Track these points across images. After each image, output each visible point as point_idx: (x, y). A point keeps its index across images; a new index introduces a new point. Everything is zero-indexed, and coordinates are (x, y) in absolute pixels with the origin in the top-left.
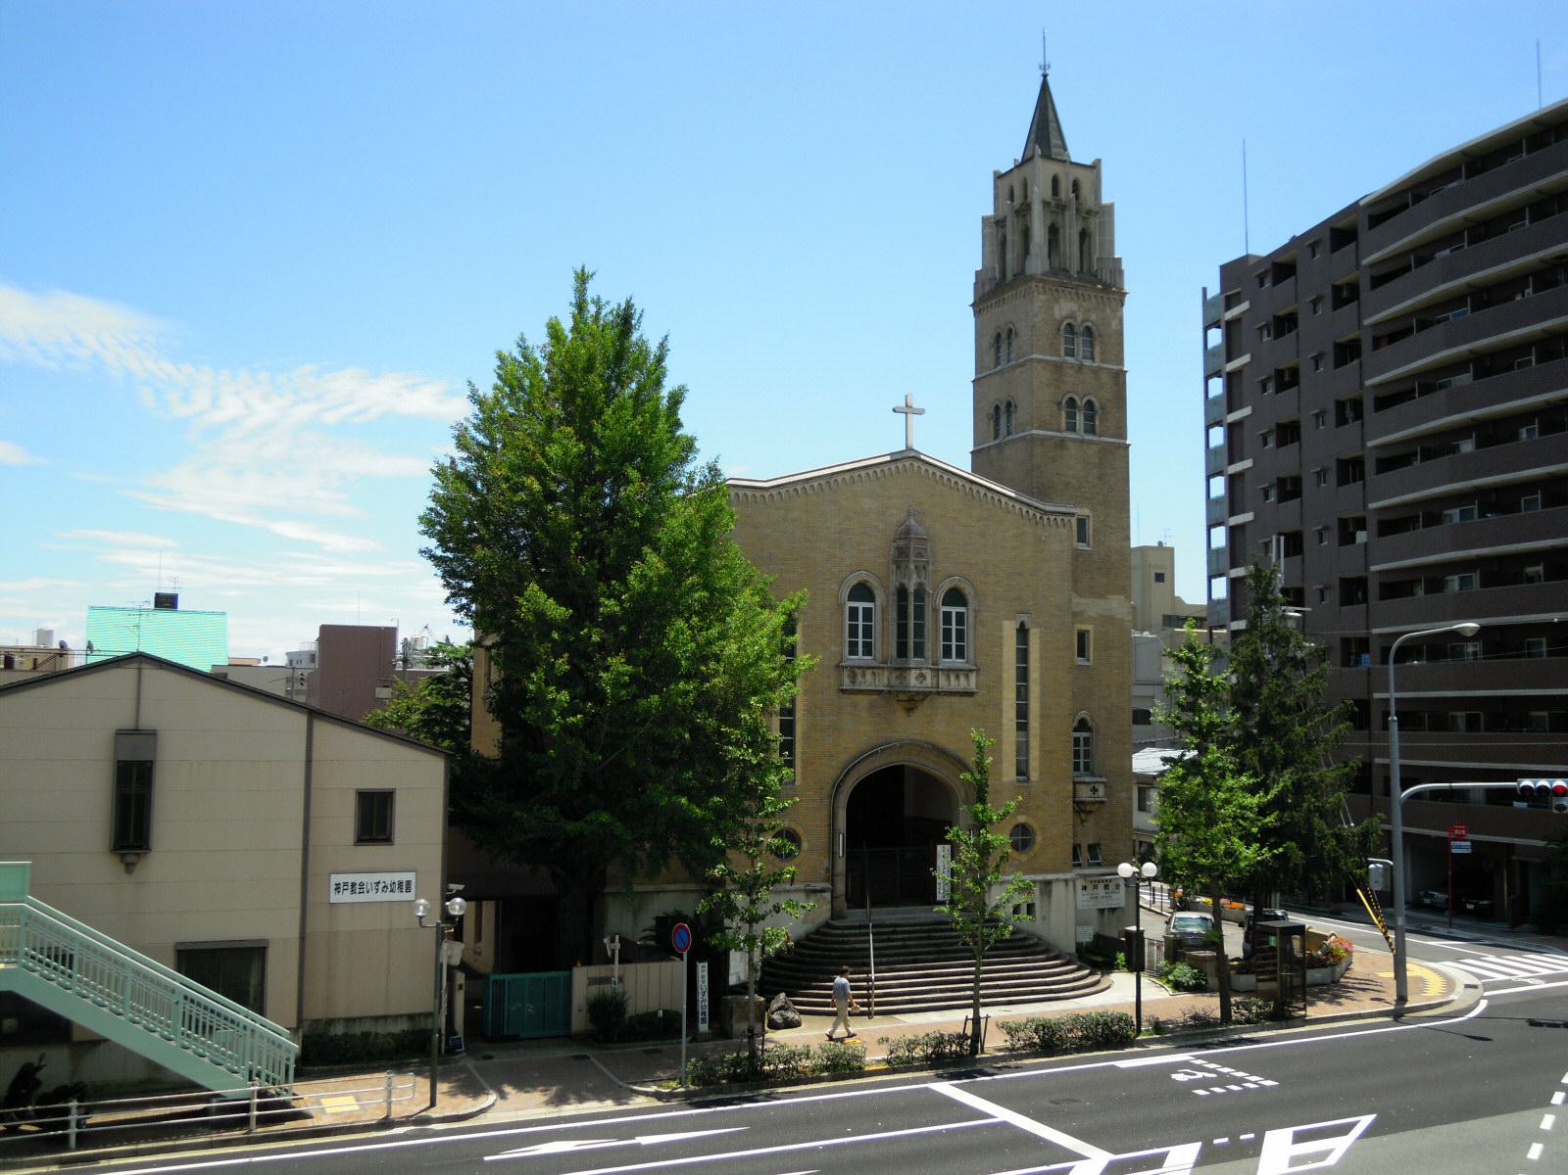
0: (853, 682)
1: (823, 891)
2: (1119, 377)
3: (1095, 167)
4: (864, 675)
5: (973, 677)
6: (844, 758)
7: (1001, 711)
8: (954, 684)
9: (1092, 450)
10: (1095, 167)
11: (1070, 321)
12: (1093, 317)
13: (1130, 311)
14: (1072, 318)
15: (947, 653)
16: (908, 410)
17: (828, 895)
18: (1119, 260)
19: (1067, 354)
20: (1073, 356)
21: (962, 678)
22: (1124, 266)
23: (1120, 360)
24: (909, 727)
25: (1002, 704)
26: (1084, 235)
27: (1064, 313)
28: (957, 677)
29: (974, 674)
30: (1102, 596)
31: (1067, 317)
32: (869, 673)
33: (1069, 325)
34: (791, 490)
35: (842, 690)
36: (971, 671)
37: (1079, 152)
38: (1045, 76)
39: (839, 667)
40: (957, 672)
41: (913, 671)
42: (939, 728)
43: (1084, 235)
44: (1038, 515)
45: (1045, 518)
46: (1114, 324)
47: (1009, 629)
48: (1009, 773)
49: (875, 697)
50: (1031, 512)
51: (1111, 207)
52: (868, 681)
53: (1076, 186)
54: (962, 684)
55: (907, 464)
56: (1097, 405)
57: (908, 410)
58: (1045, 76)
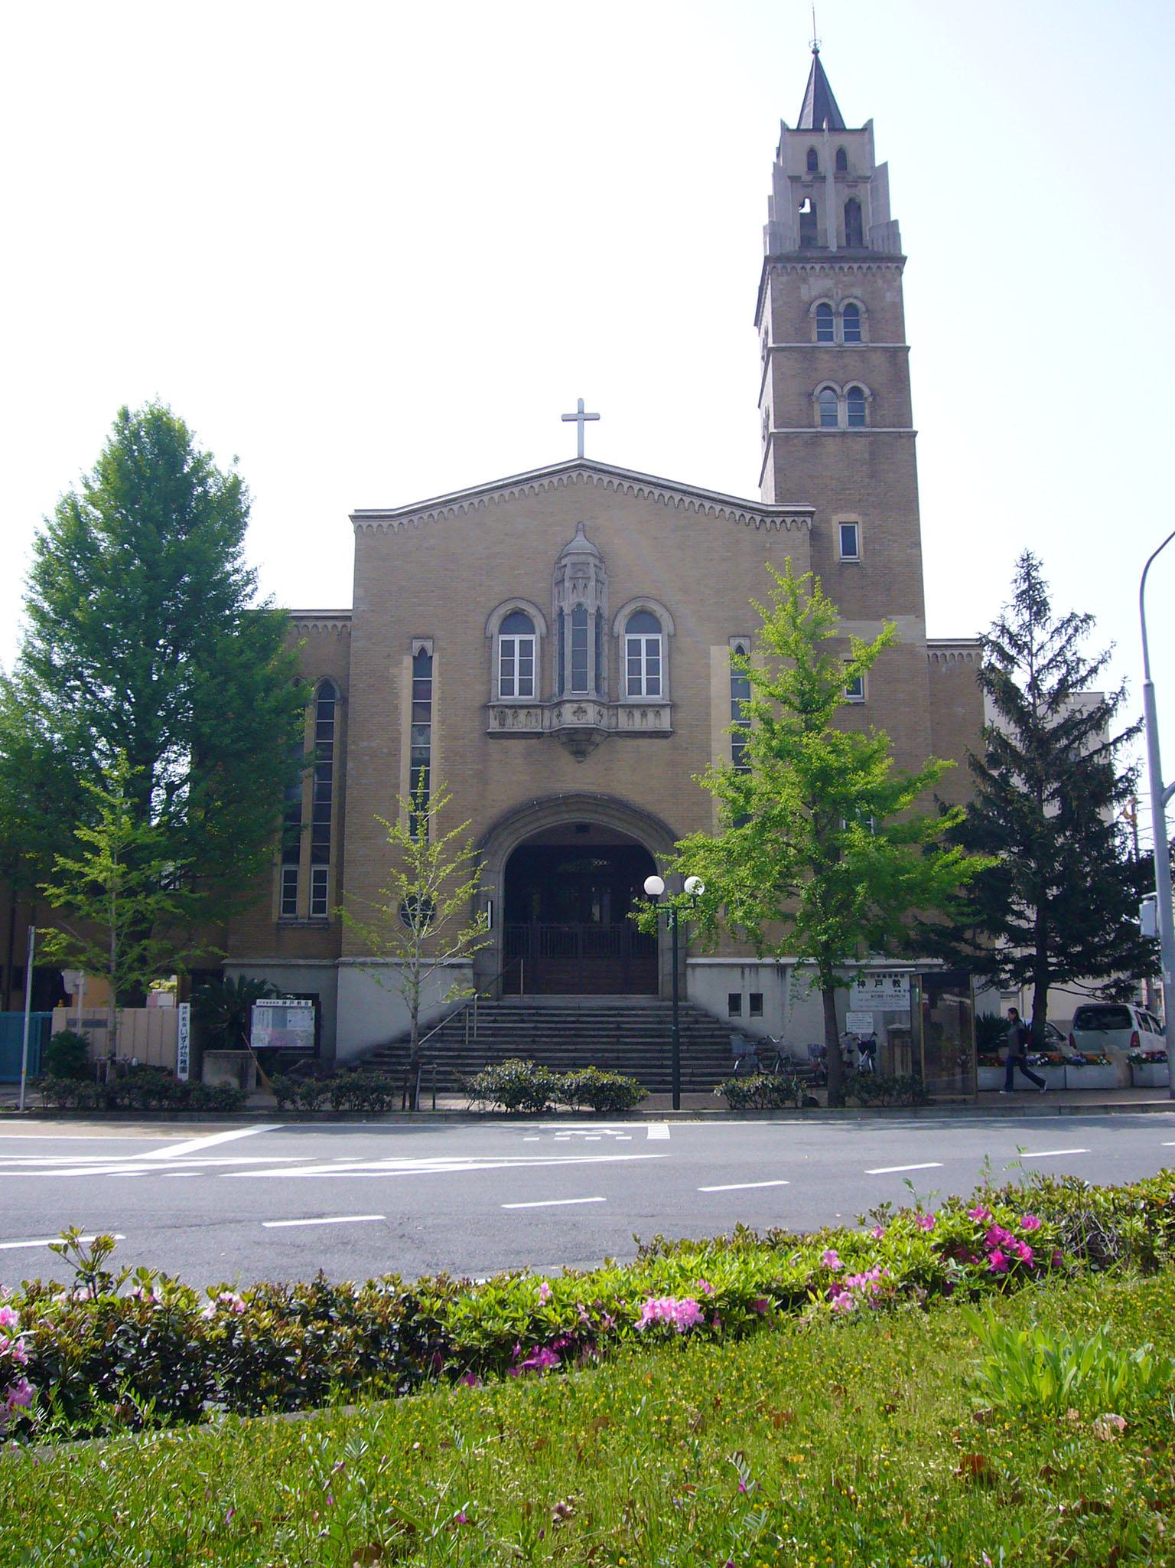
0: (502, 725)
1: (460, 966)
2: (898, 357)
3: (867, 129)
4: (515, 717)
5: (666, 714)
6: (493, 813)
8: (638, 724)
9: (860, 446)
10: (867, 129)
12: (857, 291)
14: (827, 296)
15: (634, 688)
16: (581, 417)
17: (469, 973)
18: (896, 222)
21: (651, 716)
22: (902, 229)
23: (901, 336)
24: (577, 777)
27: (814, 293)
28: (644, 715)
29: (668, 711)
31: (820, 297)
35: (493, 735)
36: (663, 706)
37: (852, 120)
38: (816, 52)
39: (486, 707)
40: (644, 708)
41: (568, 705)
42: (625, 777)
44: (758, 519)
45: (768, 520)
46: (889, 297)
49: (534, 741)
50: (748, 516)
51: (885, 166)
52: (522, 723)
53: (841, 155)
54: (651, 723)
55: (574, 475)
56: (866, 391)
57: (581, 417)
58: (816, 52)
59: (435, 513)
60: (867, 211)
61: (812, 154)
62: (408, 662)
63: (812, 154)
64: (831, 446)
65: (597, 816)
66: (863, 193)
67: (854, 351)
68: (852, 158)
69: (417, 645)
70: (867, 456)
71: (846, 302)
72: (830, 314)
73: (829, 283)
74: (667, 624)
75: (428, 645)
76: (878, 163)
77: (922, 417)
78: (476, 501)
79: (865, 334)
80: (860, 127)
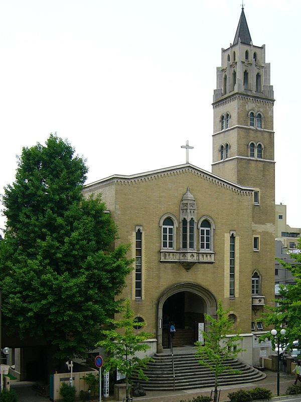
0: (165, 258)
2: (272, 134)
3: (263, 48)
6: (162, 289)
7: (224, 269)
8: (205, 259)
10: (263, 48)
11: (253, 111)
12: (261, 110)
13: (277, 108)
16: (187, 147)
17: (155, 344)
19: (251, 125)
20: (253, 126)
24: (187, 277)
25: (224, 267)
26: (258, 76)
28: (207, 256)
29: (213, 255)
30: (263, 223)
32: (171, 254)
33: (252, 113)
34: (181, 170)
35: (161, 262)
36: (212, 253)
37: (256, 41)
38: (243, 9)
41: (189, 254)
42: (200, 277)
43: (258, 76)
44: (239, 191)
47: (227, 237)
48: (227, 294)
49: (174, 264)
51: (269, 64)
52: (171, 258)
54: (208, 259)
56: (263, 146)
57: (187, 147)
58: (243, 9)
59: (143, 179)
60: (263, 78)
61: (247, 52)
62: (134, 234)
63: (247, 52)
64: (253, 164)
65: (190, 289)
66: (262, 72)
67: (260, 131)
68: (258, 57)
69: (137, 228)
70: (262, 169)
71: (258, 113)
72: (253, 116)
73: (254, 105)
74: (213, 227)
75: (141, 228)
76: (266, 62)
77: (277, 158)
78: (156, 176)
79: (263, 126)
80: (260, 46)
